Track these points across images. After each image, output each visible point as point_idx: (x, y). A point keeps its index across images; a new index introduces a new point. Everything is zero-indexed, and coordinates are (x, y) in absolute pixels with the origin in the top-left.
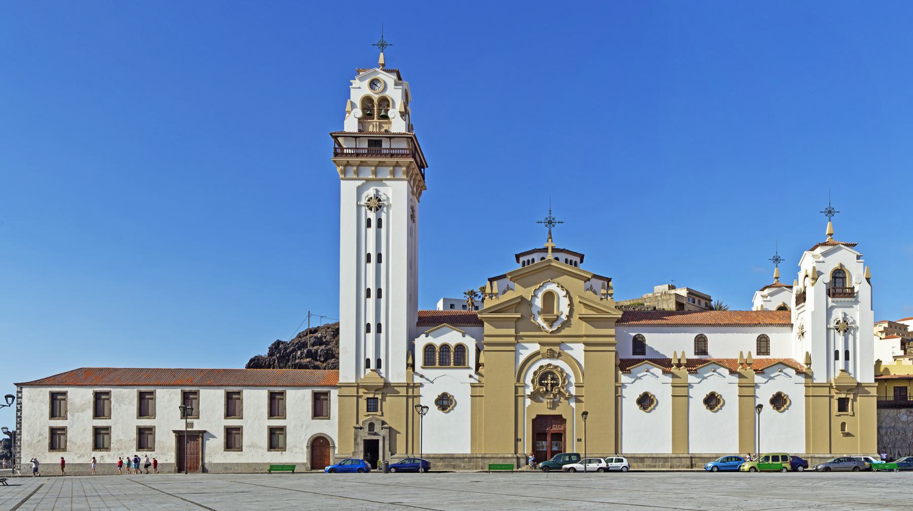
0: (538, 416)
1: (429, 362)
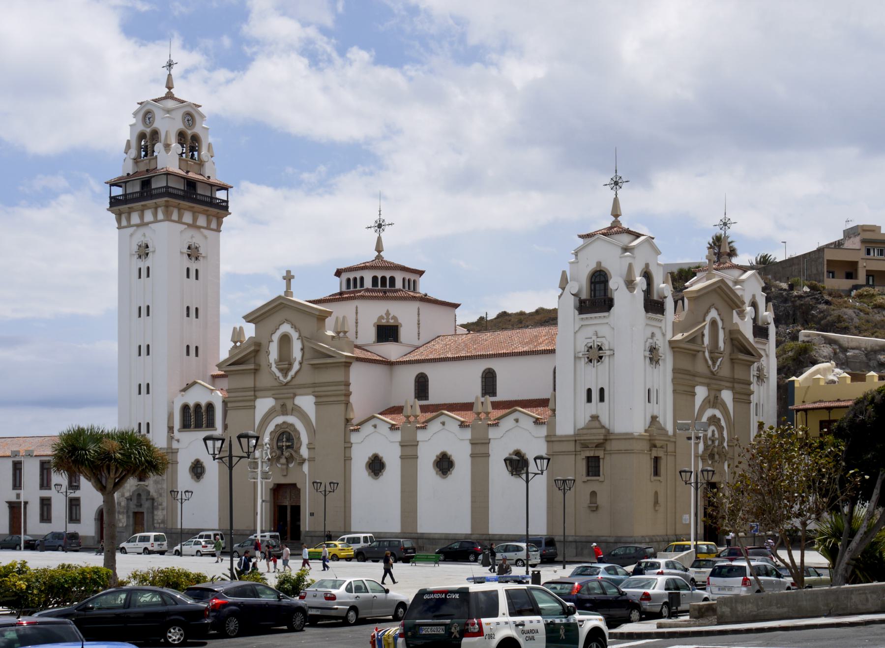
1: (185, 426)
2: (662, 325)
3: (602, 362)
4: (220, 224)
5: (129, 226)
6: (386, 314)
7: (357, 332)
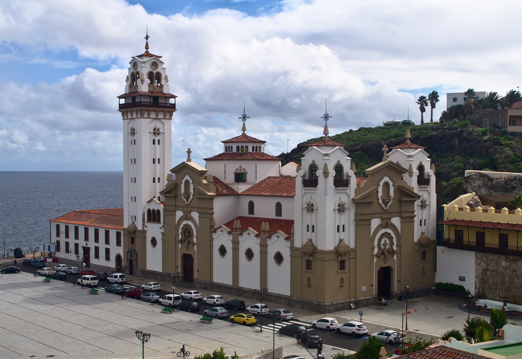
2: (348, 191)
3: (313, 212)
4: (171, 116)
5: (127, 119)
6: (239, 167)
7: (225, 177)
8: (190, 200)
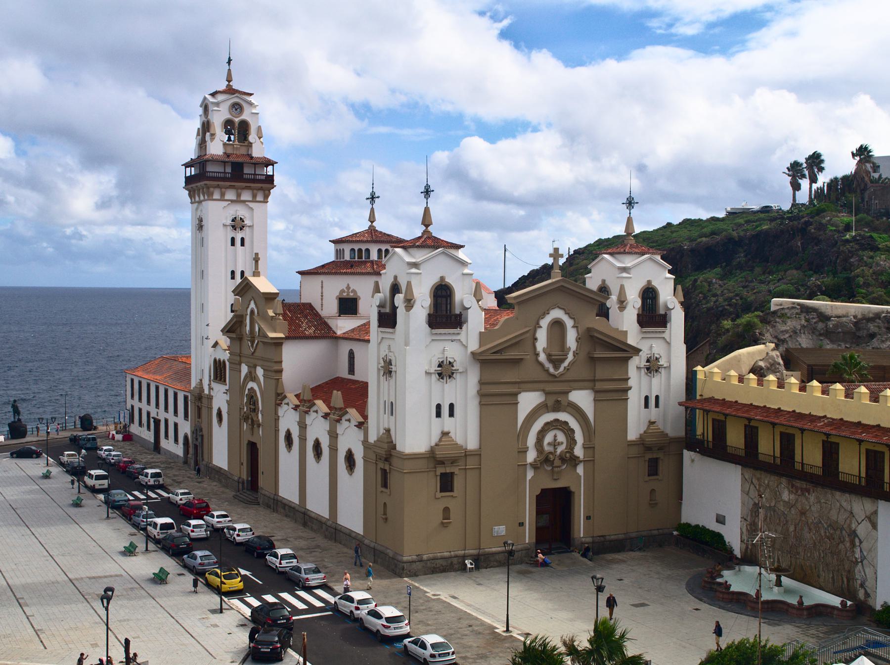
0: (543, 490)
8: (566, 364)
